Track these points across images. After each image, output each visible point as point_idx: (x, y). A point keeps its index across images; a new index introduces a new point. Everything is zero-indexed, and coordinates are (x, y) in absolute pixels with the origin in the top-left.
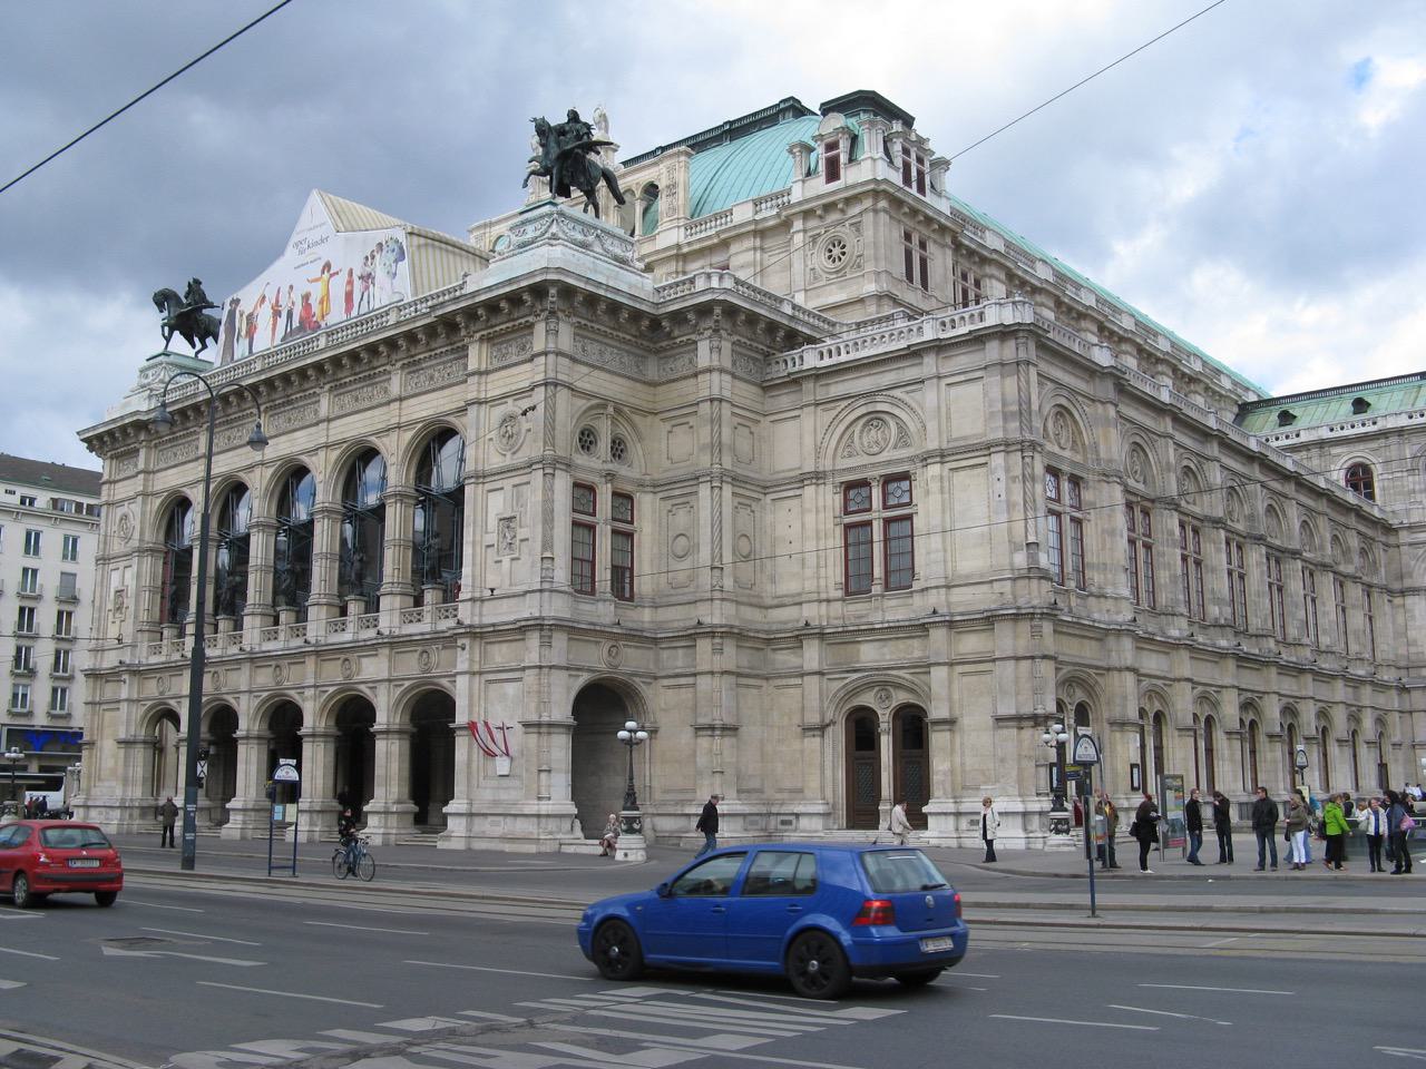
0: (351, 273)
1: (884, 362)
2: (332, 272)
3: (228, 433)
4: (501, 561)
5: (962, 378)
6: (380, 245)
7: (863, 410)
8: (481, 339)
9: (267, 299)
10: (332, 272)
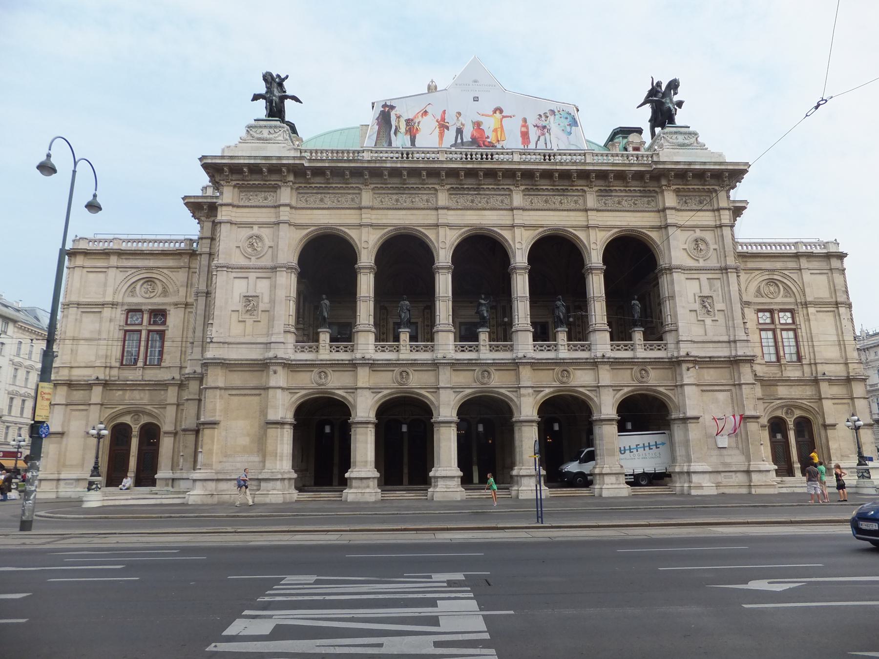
0: (525, 120)
1: (778, 257)
2: (504, 114)
3: (395, 197)
4: (703, 321)
5: (818, 271)
6: (553, 112)
7: (767, 277)
8: (674, 191)
9: (429, 117)
10: (504, 114)
